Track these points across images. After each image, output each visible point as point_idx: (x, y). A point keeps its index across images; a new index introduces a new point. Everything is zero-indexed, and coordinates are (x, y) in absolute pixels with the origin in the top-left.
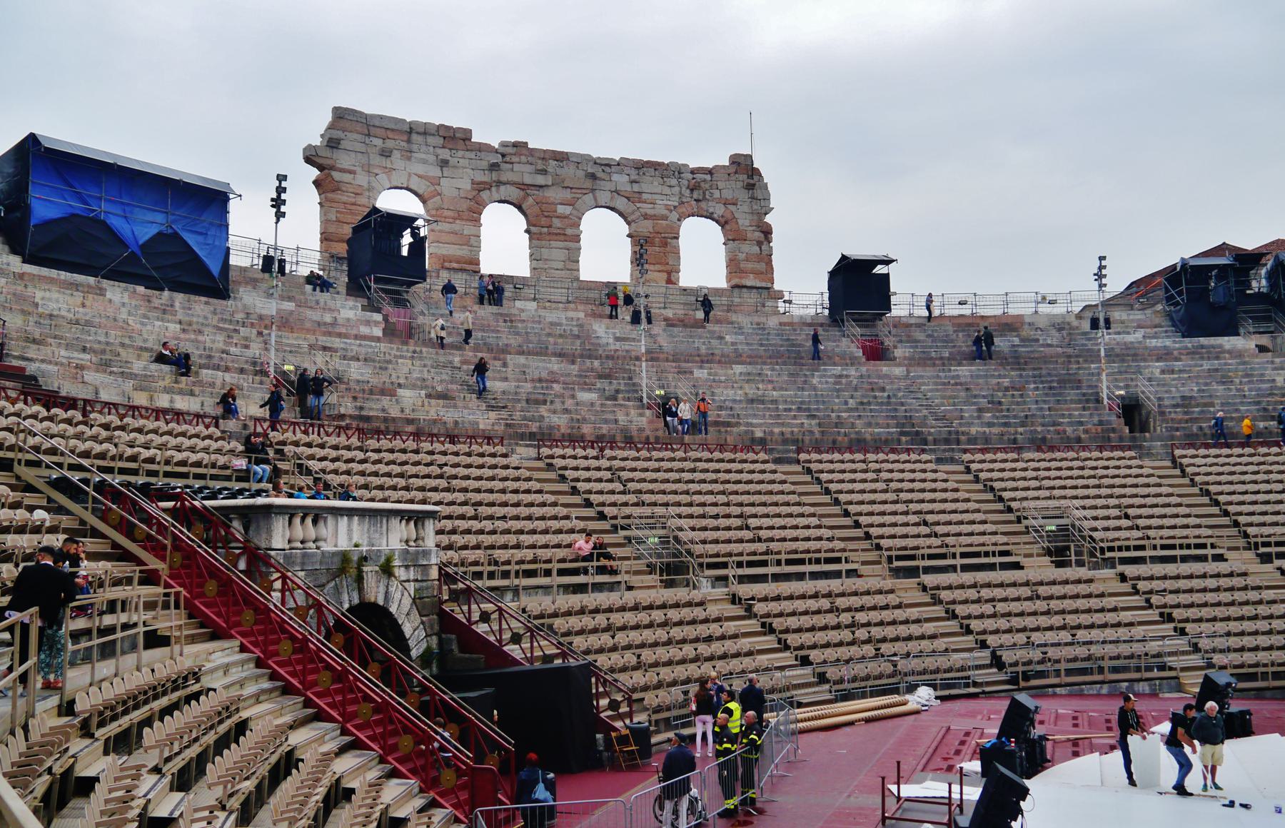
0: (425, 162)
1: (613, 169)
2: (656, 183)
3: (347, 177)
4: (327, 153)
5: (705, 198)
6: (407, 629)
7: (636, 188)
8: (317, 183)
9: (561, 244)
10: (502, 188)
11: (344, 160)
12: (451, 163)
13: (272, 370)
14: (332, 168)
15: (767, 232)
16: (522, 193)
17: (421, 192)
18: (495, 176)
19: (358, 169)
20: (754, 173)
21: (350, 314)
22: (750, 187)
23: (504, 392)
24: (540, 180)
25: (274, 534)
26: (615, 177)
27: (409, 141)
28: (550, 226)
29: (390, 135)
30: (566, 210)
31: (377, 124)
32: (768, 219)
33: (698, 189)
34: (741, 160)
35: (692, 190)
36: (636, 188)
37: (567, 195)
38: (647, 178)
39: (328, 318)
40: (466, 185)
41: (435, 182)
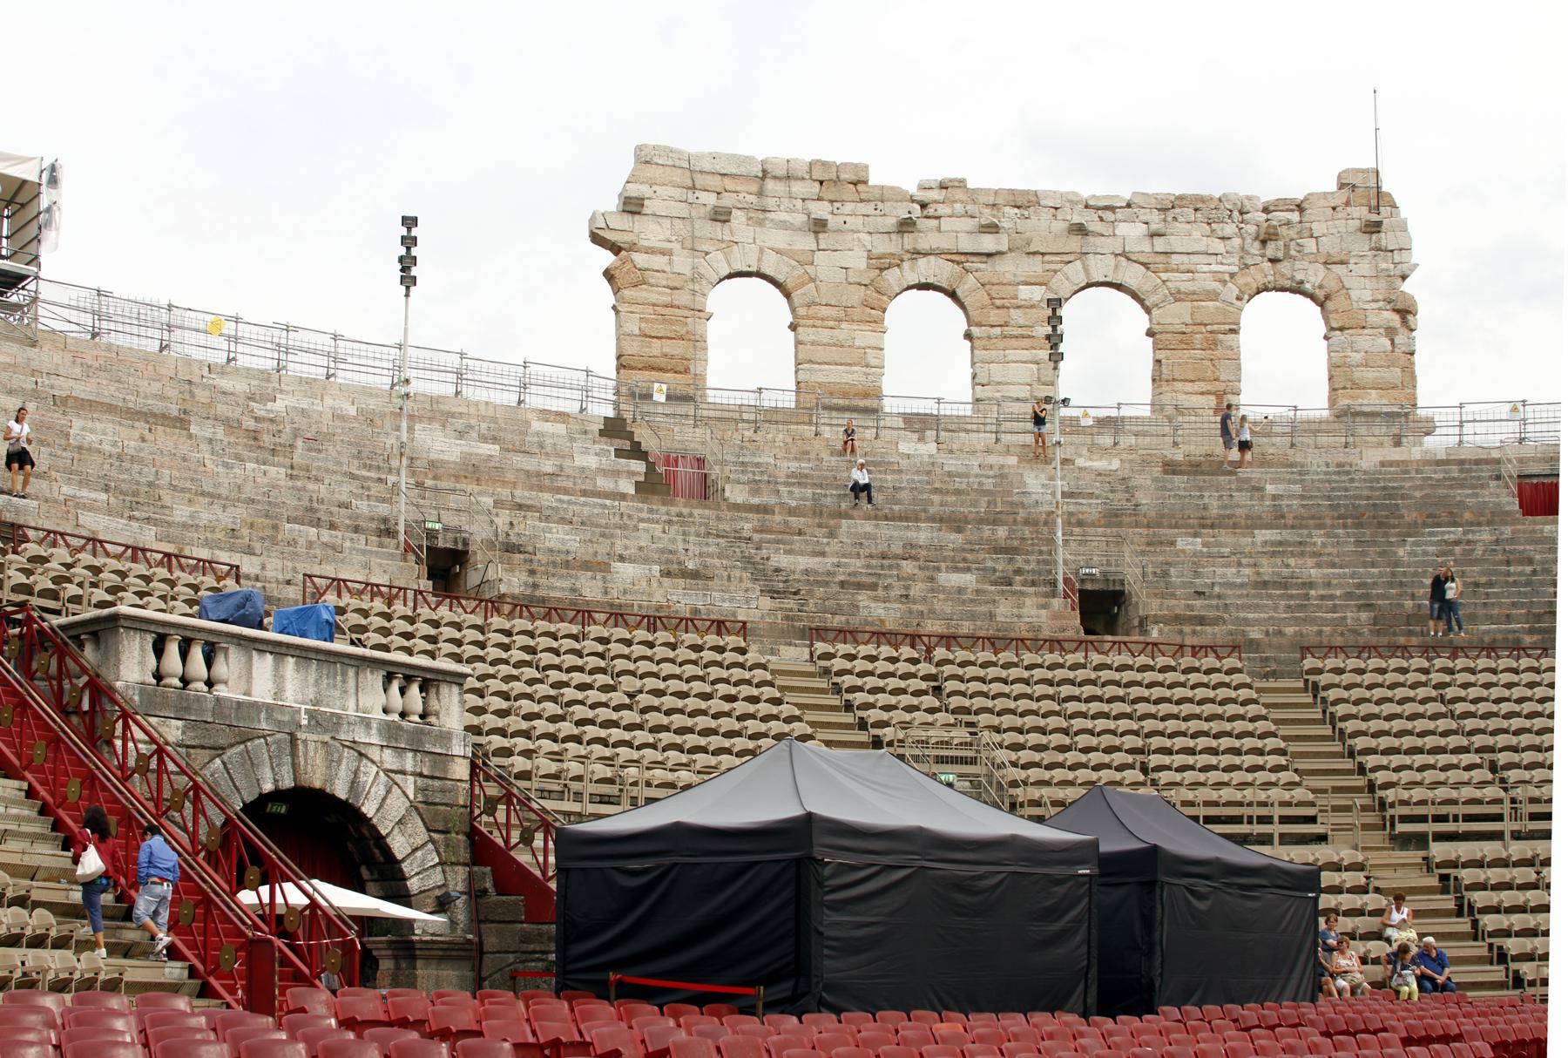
0: (784, 226)
1: (1120, 214)
2: (1196, 235)
3: (658, 262)
4: (625, 222)
5: (1287, 256)
6: (399, 845)
8: (609, 275)
9: (1025, 355)
10: (922, 261)
11: (650, 232)
12: (833, 222)
13: (401, 529)
14: (633, 247)
15: (1405, 312)
17: (780, 278)
18: (909, 241)
19: (676, 247)
20: (1379, 199)
21: (592, 462)
22: (1373, 228)
23: (806, 572)
24: (988, 243)
25: (124, 657)
26: (1123, 229)
31: (707, 167)
32: (1406, 287)
33: (1272, 243)
34: (1357, 181)
35: (1264, 242)
36: (1160, 244)
37: (1035, 266)
38: (1181, 227)
39: (548, 466)
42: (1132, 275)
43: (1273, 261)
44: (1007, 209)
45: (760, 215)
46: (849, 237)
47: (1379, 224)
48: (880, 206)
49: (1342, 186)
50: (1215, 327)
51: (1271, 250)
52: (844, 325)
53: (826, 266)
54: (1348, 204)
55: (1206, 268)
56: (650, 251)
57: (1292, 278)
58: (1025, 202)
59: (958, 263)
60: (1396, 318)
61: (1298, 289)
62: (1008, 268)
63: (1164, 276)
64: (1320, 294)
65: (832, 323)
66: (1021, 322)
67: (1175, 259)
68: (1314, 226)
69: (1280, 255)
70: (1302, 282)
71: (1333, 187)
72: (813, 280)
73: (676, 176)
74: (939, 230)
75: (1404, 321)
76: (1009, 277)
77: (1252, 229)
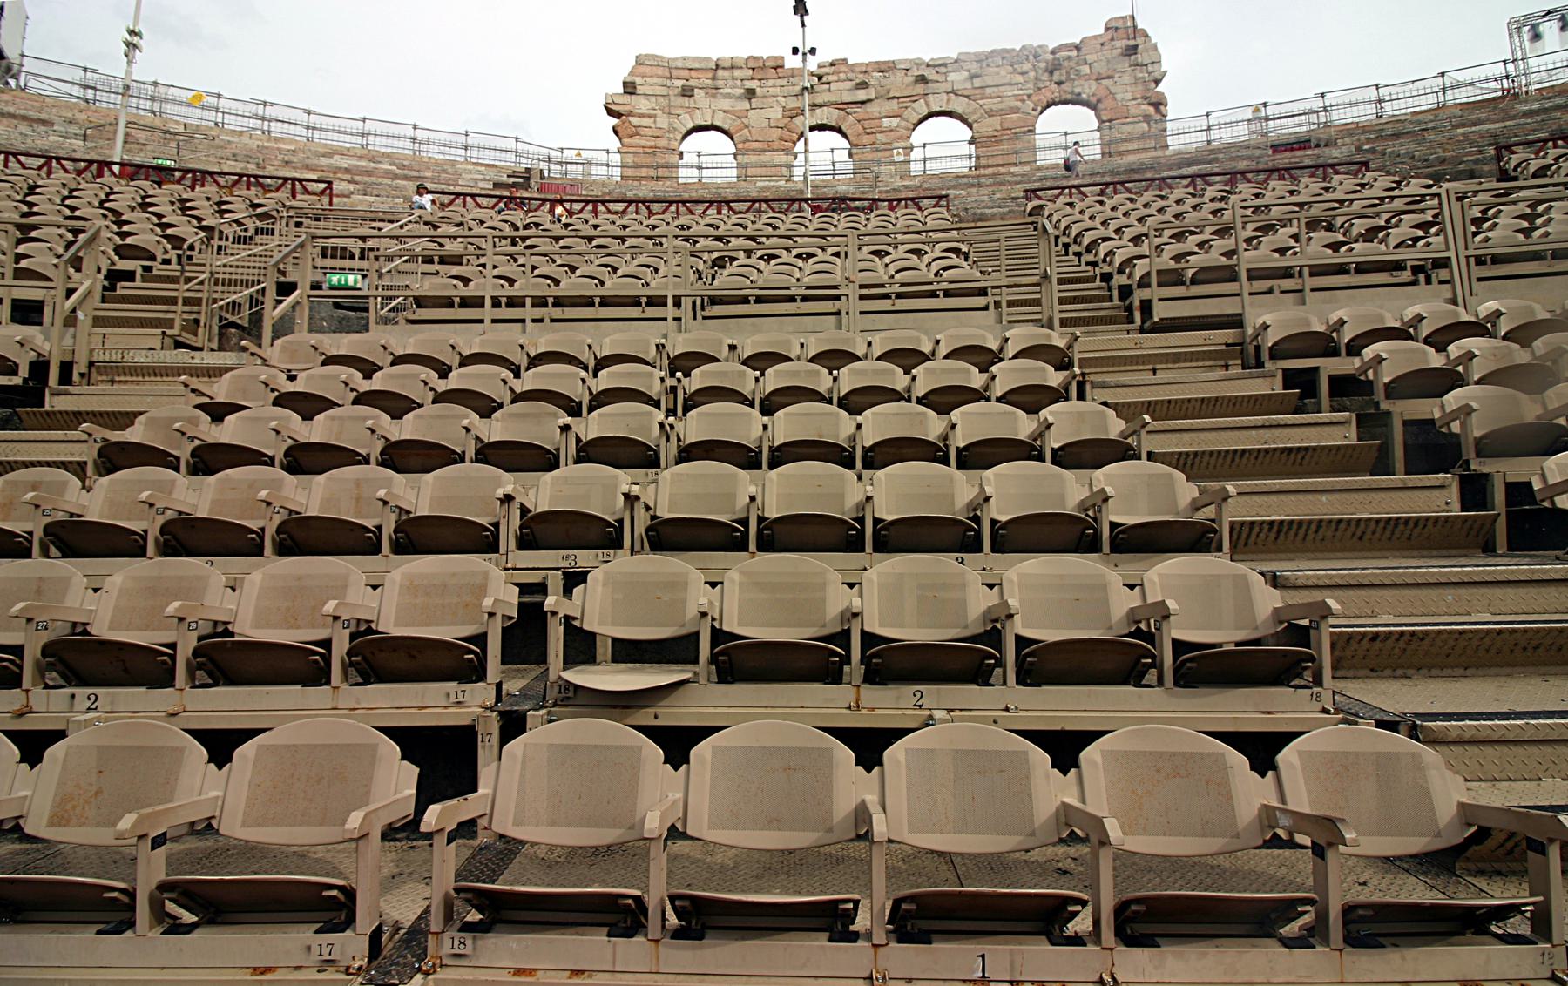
0: (728, 96)
3: (646, 122)
5: (1069, 79)
7: (977, 82)
10: (819, 111)
11: (641, 104)
12: (758, 90)
14: (630, 114)
15: (1159, 104)
17: (726, 127)
19: (659, 112)
20: (1136, 31)
22: (1132, 50)
24: (862, 95)
27: (714, 78)
29: (693, 74)
30: (895, 122)
33: (1059, 74)
34: (1120, 24)
35: (1051, 73)
36: (977, 82)
40: (777, 113)
41: (743, 115)
42: (958, 105)
43: (1059, 83)
47: (1136, 47)
49: (1107, 29)
51: (1056, 77)
56: (641, 116)
58: (886, 68)
60: (1152, 109)
62: (873, 109)
64: (1093, 100)
67: (988, 91)
71: (1101, 31)
73: (660, 71)
75: (1158, 111)
77: (1043, 65)
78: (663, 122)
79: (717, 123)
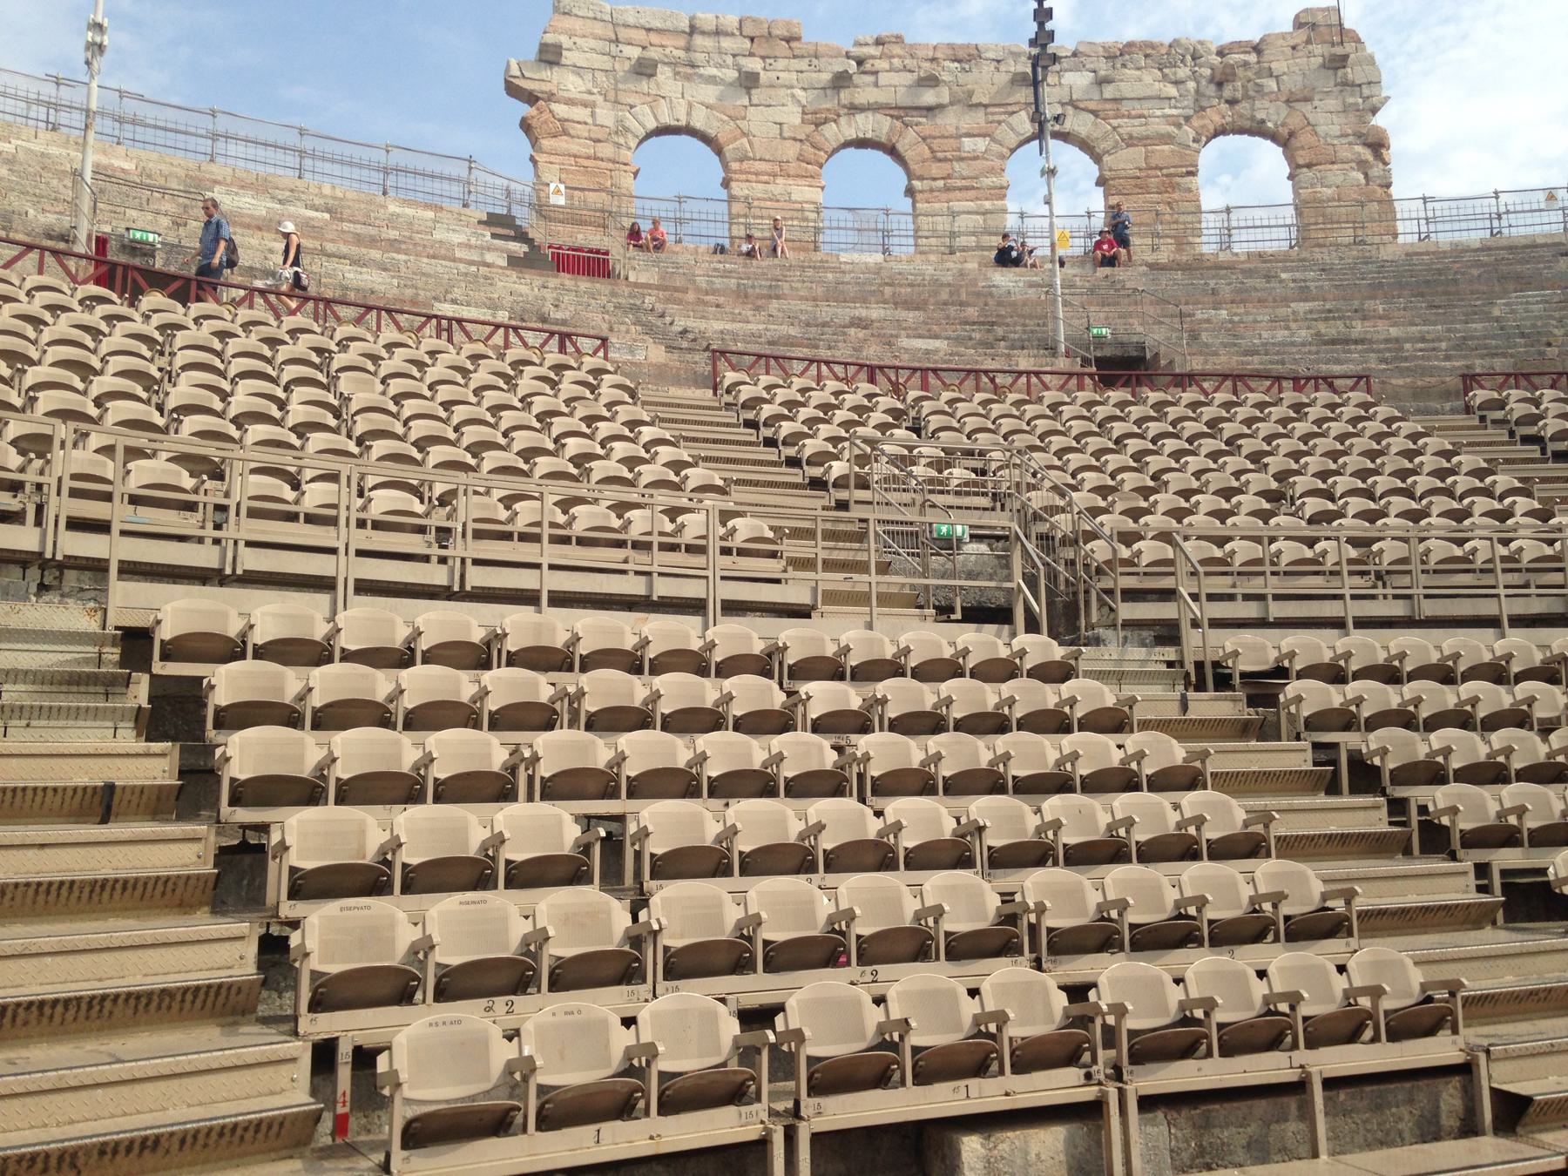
0: (712, 80)
3: (580, 113)
8: (526, 126)
10: (860, 118)
14: (551, 97)
15: (1378, 145)
16: (898, 124)
17: (712, 132)
18: (845, 96)
19: (599, 99)
20: (1344, 35)
22: (1337, 63)
24: (929, 97)
27: (688, 49)
28: (949, 177)
29: (654, 38)
30: (981, 144)
32: (1379, 120)
33: (1229, 88)
34: (1320, 18)
35: (1220, 85)
36: (1109, 91)
37: (977, 119)
40: (792, 116)
43: (1232, 102)
44: (947, 64)
45: (689, 70)
46: (783, 92)
47: (1345, 57)
48: (815, 62)
49: (1299, 24)
50: (1172, 170)
51: (1228, 92)
52: (780, 180)
53: (759, 121)
54: (1308, 42)
55: (1158, 113)
56: (570, 102)
57: (1253, 118)
59: (898, 118)
61: (1257, 129)
62: (950, 121)
63: (1115, 122)
64: (1284, 132)
65: (765, 178)
66: (965, 173)
68: (1273, 65)
69: (1239, 95)
70: (1263, 122)
71: (1288, 27)
72: (744, 134)
73: (598, 29)
74: (876, 85)
75: (1378, 156)
76: (952, 130)
78: (606, 115)
79: (698, 124)
